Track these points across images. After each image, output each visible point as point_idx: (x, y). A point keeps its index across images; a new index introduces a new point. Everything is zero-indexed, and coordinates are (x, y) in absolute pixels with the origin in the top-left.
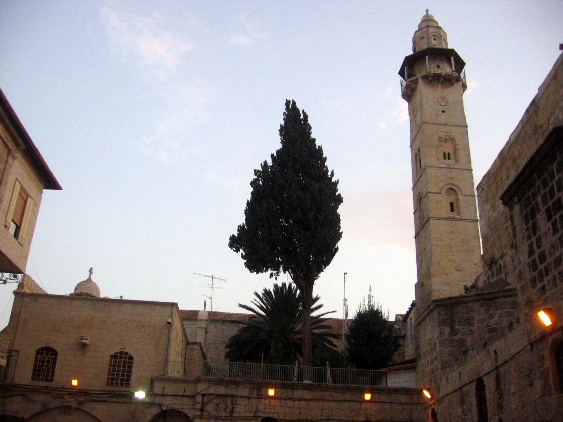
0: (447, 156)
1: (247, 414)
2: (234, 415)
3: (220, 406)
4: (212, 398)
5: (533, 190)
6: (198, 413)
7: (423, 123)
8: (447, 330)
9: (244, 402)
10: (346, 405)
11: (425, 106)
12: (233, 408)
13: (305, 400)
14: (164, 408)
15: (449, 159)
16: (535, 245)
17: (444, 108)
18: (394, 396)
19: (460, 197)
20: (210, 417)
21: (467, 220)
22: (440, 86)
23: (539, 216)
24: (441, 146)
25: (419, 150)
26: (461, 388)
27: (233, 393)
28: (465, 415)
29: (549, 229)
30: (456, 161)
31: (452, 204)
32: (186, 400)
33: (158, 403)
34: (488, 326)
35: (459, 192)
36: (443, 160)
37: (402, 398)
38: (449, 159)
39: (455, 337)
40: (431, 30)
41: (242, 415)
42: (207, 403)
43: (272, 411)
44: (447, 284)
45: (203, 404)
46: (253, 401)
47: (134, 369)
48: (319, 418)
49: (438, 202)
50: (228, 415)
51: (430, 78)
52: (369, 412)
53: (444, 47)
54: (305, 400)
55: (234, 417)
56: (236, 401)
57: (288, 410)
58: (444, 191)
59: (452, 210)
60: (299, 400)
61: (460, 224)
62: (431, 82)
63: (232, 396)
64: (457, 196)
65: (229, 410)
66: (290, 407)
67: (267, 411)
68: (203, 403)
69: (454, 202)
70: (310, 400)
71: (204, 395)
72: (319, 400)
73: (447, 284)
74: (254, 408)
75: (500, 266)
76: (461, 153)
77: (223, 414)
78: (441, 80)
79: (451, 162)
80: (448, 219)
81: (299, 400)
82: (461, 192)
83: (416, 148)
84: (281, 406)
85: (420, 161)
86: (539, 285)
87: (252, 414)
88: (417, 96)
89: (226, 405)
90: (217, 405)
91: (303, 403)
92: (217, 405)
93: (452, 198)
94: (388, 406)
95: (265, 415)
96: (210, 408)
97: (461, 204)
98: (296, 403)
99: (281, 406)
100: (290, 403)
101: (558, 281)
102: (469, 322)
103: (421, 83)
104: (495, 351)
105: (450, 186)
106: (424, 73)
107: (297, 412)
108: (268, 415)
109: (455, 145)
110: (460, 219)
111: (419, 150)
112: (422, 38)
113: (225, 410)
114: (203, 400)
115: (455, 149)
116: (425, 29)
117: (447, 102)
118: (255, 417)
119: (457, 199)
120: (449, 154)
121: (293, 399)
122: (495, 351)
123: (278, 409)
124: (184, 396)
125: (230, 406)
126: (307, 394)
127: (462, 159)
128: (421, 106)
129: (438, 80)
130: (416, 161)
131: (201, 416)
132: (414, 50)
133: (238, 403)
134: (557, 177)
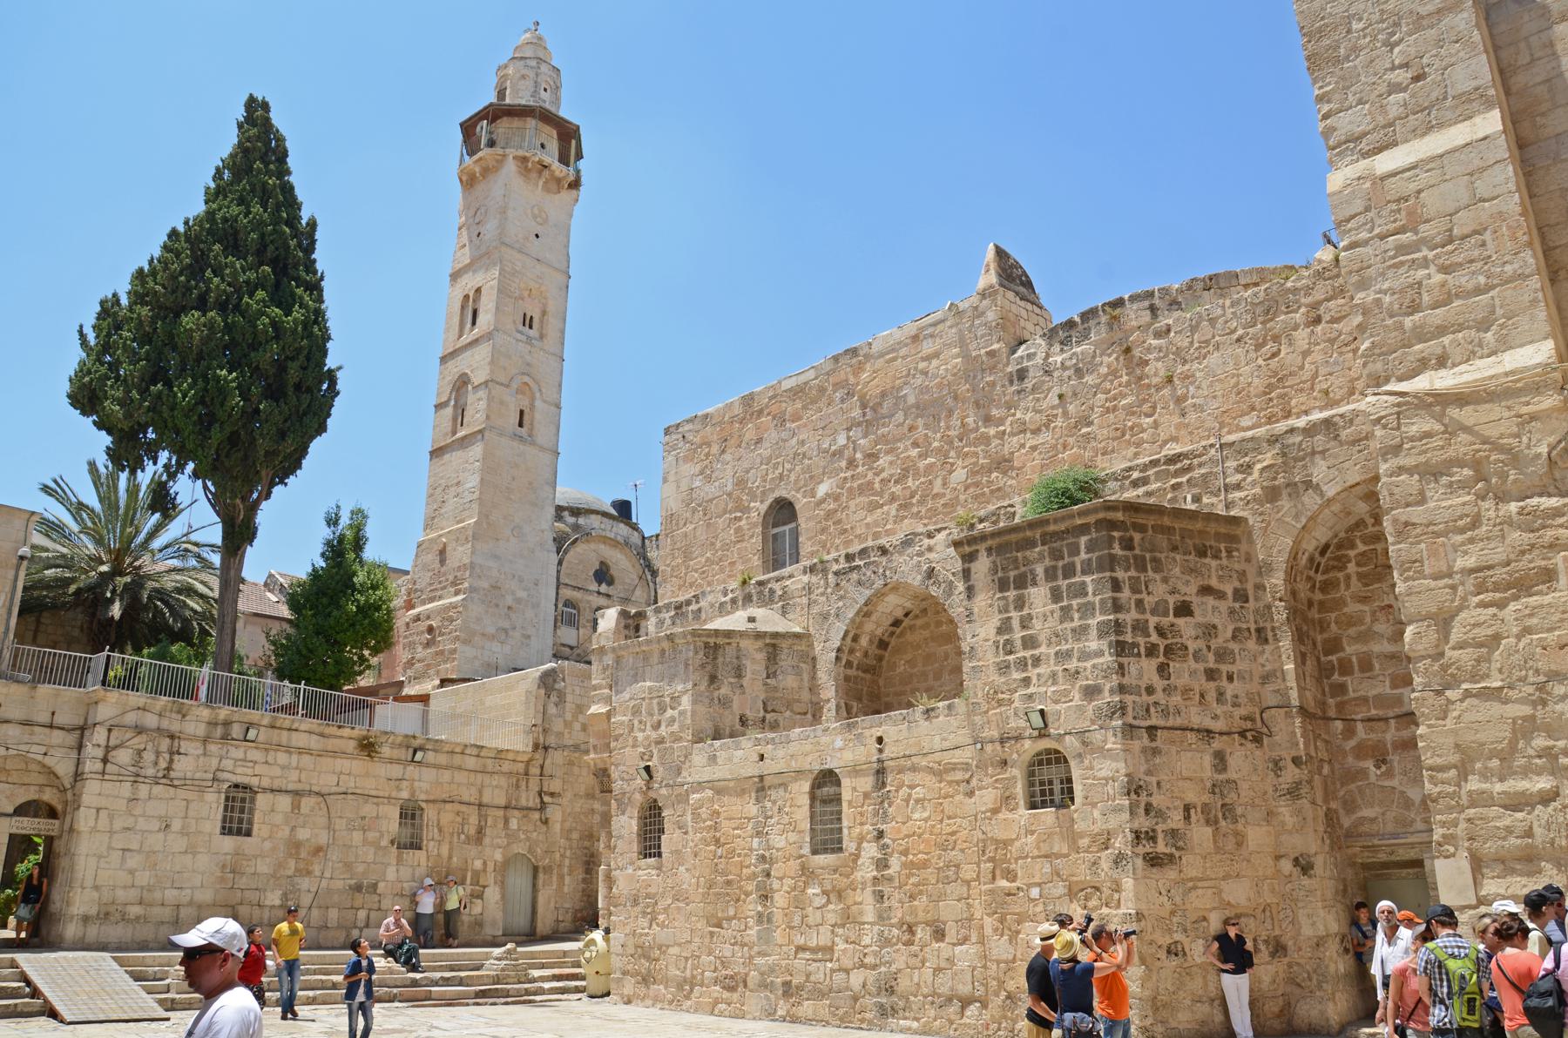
0: (528, 322)
1: (198, 775)
3: (145, 755)
5: (1028, 553)
6: (99, 766)
7: (503, 243)
8: (705, 683)
11: (510, 213)
12: (171, 761)
16: (1016, 624)
17: (538, 229)
18: (457, 760)
19: (538, 403)
21: (542, 449)
23: (1032, 590)
25: (478, 290)
26: (761, 777)
27: (175, 727)
28: (767, 818)
29: (1052, 612)
30: (542, 337)
31: (522, 412)
32: (57, 737)
34: (766, 684)
36: (521, 327)
39: (716, 694)
40: (544, 68)
41: (189, 775)
42: (116, 747)
43: (249, 771)
44: (496, 557)
46: (213, 748)
48: (334, 789)
49: (502, 403)
53: (553, 109)
57: (277, 771)
58: (514, 385)
59: (521, 425)
60: (302, 751)
62: (528, 170)
64: (533, 399)
65: (163, 765)
66: (283, 768)
67: (239, 770)
69: (527, 411)
72: (334, 754)
73: (496, 557)
74: (214, 762)
75: (772, 591)
76: (552, 323)
77: (150, 772)
78: (546, 173)
79: (533, 333)
81: (302, 751)
83: (469, 283)
85: (475, 313)
86: (1017, 675)
89: (158, 754)
91: (306, 759)
93: (525, 403)
94: (446, 776)
96: (123, 757)
97: (538, 416)
98: (295, 757)
100: (282, 758)
101: (1061, 680)
102: (739, 673)
103: (511, 166)
104: (880, 740)
105: (526, 379)
106: (521, 153)
107: (294, 776)
109: (545, 305)
110: (533, 443)
111: (478, 290)
112: (523, 77)
115: (544, 313)
116: (533, 63)
117: (546, 221)
119: (532, 407)
121: (288, 749)
122: (880, 740)
123: (259, 769)
124: (51, 727)
125: (167, 756)
126: (314, 742)
127: (552, 333)
128: (503, 211)
130: (463, 308)
131: (103, 773)
132: (501, 94)
134: (1083, 556)
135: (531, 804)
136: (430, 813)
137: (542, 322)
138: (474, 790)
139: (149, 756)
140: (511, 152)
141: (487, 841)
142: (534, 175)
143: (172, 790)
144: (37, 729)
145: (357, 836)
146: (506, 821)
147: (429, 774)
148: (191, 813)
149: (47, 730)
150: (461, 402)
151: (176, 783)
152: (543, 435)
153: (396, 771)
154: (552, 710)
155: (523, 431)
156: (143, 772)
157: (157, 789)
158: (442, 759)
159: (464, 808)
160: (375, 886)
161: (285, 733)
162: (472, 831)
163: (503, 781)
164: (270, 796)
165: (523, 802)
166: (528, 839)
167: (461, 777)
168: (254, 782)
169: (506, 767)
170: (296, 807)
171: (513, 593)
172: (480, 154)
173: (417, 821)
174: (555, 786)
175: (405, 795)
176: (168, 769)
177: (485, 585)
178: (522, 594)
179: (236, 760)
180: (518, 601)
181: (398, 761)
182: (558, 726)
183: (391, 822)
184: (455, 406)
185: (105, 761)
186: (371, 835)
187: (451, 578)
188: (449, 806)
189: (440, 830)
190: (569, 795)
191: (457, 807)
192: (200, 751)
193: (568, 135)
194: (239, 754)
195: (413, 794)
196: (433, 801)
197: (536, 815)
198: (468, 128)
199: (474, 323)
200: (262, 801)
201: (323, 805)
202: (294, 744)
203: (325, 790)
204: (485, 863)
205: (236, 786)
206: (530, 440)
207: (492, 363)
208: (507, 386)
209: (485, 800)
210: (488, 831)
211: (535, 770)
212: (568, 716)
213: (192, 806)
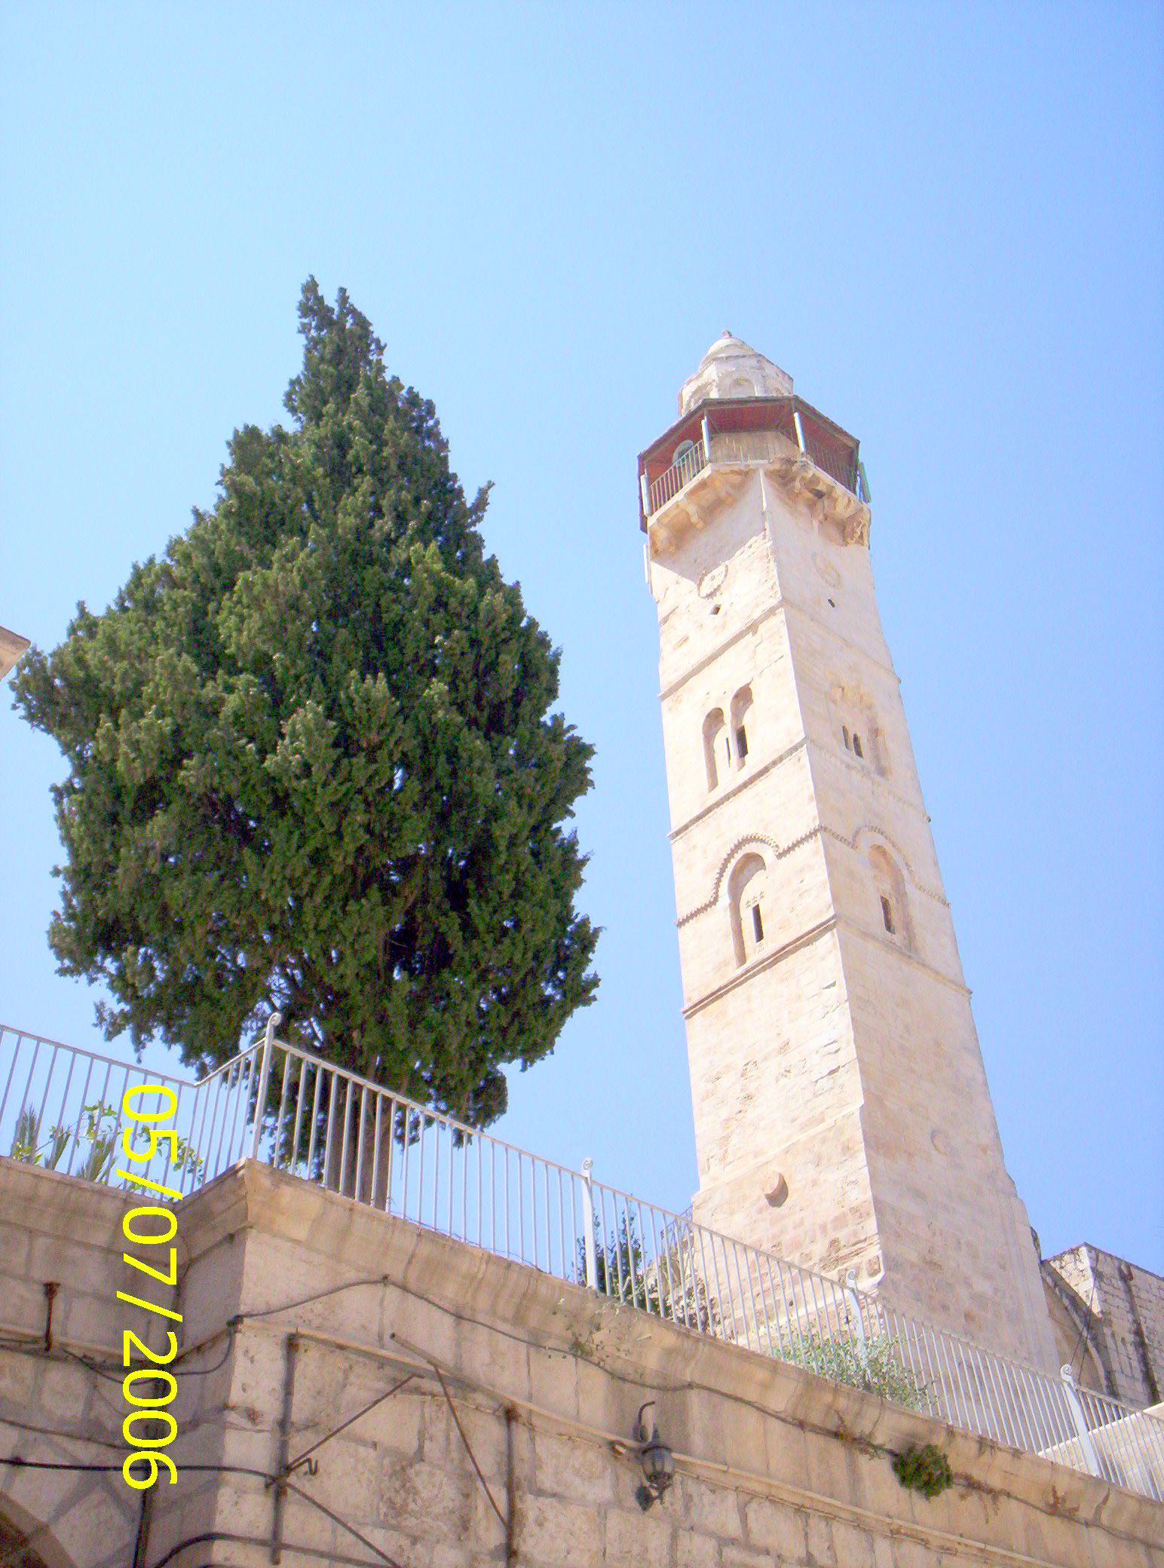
15: (859, 753)
17: (830, 592)
19: (910, 888)
22: (815, 523)
24: (834, 702)
25: (743, 697)
35: (905, 872)
38: (859, 753)
44: (919, 1195)
51: (797, 484)
59: (889, 927)
69: (892, 902)
73: (919, 1195)
79: (867, 760)
80: (891, 946)
82: (911, 872)
85: (741, 737)
90: (402, 1467)
92: (402, 1467)
97: (917, 914)
105: (880, 840)
111: (743, 697)
115: (875, 732)
119: (902, 895)
120: (856, 739)
129: (811, 506)
130: (709, 737)
137: (875, 748)
142: (802, 508)
150: (749, 894)
155: (897, 938)
171: (968, 1284)
172: (706, 473)
177: (913, 1256)
178: (982, 1286)
180: (978, 1299)
184: (735, 908)
185: (277, 1484)
187: (819, 1249)
193: (837, 452)
199: (743, 751)
207: (819, 796)
208: (853, 845)
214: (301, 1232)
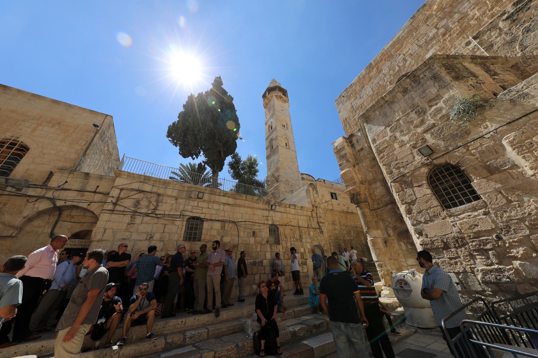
2: (157, 212)
4: (133, 193)
9: (172, 201)
10: (259, 212)
12: (157, 205)
13: (229, 205)
14: (59, 203)
18: (288, 209)
20: (123, 213)
27: (161, 191)
33: (52, 197)
37: (293, 211)
41: (167, 213)
43: (200, 211)
45: (118, 199)
46: (181, 201)
47: (24, 161)
50: (150, 212)
52: (274, 218)
54: (229, 205)
55: (156, 214)
56: (163, 199)
57: (214, 212)
61: (290, 151)
62: (278, 98)
63: (159, 195)
65: (152, 207)
66: (217, 210)
67: (194, 211)
68: (119, 197)
70: (233, 205)
71: (121, 190)
72: (240, 206)
74: (181, 207)
77: (144, 211)
81: (225, 204)
84: (208, 208)
87: (179, 213)
88: (272, 102)
91: (227, 207)
95: (191, 215)
98: (222, 207)
99: (208, 208)
100: (216, 206)
103: (274, 97)
108: (195, 215)
113: (148, 207)
114: (120, 194)
118: (182, 215)
121: (218, 203)
123: (204, 211)
125: (155, 204)
128: (274, 105)
131: (113, 210)
133: (164, 201)
135: (316, 227)
136: (281, 229)
138: (295, 221)
139: (144, 203)
140: (274, 95)
141: (304, 240)
143: (156, 220)
144: (86, 193)
145: (252, 240)
146: (309, 234)
147: (278, 215)
148: (166, 230)
149: (93, 194)
151: (159, 216)
152: (292, 147)
153: (266, 213)
154: (315, 195)
155: (287, 147)
156: (139, 211)
157: (146, 219)
158: (282, 209)
159: (293, 228)
160: (262, 262)
161: (217, 197)
162: (298, 237)
163: (305, 218)
164: (210, 223)
165: (313, 226)
166: (318, 239)
167: (290, 216)
168: (202, 216)
169: (305, 213)
170: (223, 227)
173: (276, 233)
174: (322, 221)
175: (270, 222)
176: (155, 209)
179: (193, 206)
181: (266, 210)
182: (318, 200)
183: (265, 233)
186: (258, 239)
188: (287, 227)
189: (286, 237)
190: (327, 223)
191: (291, 227)
192: (174, 202)
193: (284, 92)
194: (195, 203)
195: (273, 221)
196: (282, 225)
197: (319, 231)
198: (264, 96)
200: (206, 225)
201: (235, 226)
202: (222, 201)
203: (235, 221)
204: (305, 250)
205: (193, 218)
206: (289, 148)
209: (300, 225)
210: (303, 236)
211: (314, 215)
212: (321, 198)
213: (167, 227)
214: (126, 177)
